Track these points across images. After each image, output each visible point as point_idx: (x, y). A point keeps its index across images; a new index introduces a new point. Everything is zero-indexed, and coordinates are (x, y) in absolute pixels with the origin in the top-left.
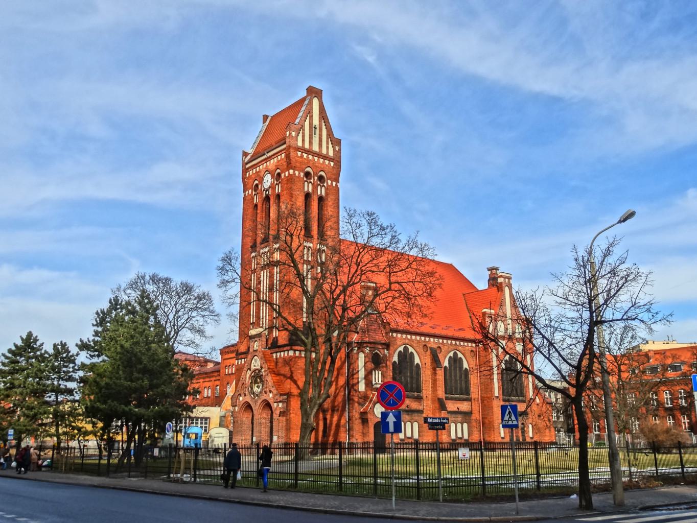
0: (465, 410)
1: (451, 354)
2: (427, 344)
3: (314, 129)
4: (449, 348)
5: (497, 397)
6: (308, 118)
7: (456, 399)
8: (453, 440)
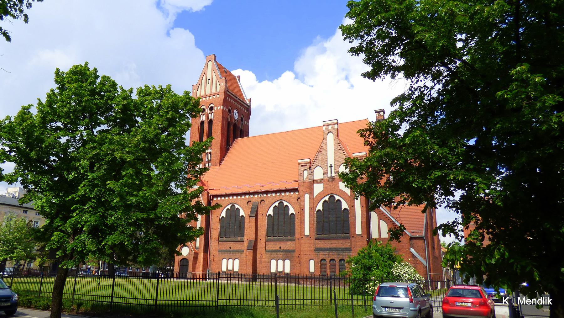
1: (277, 204)
2: (251, 201)
3: (208, 81)
5: (307, 236)
8: (274, 273)
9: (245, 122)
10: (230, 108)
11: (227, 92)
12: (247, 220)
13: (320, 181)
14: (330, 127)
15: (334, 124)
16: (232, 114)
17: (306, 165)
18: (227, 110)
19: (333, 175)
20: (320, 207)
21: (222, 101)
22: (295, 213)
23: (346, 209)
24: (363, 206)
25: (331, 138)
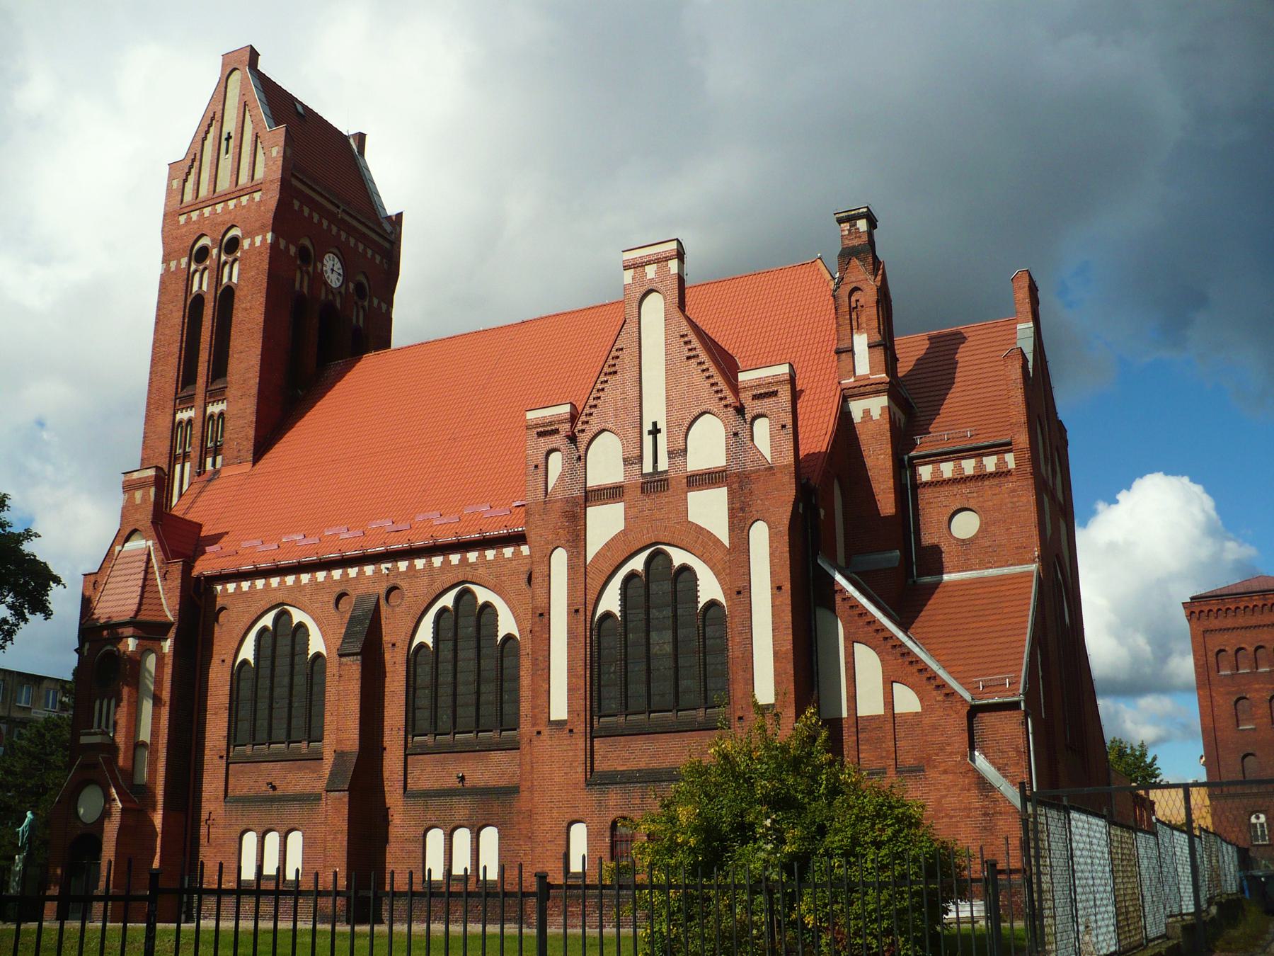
0: (492, 783)
1: (448, 600)
2: (350, 591)
3: (224, 143)
4: (432, 582)
5: (560, 724)
6: (212, 129)
7: (452, 749)
9: (376, 302)
10: (307, 242)
11: (295, 182)
12: (332, 669)
13: (611, 493)
14: (651, 271)
15: (667, 259)
16: (315, 267)
17: (556, 431)
18: (293, 250)
19: (663, 465)
20: (611, 601)
21: (271, 215)
22: (517, 635)
23: (712, 604)
24: (779, 588)
25: (655, 311)
